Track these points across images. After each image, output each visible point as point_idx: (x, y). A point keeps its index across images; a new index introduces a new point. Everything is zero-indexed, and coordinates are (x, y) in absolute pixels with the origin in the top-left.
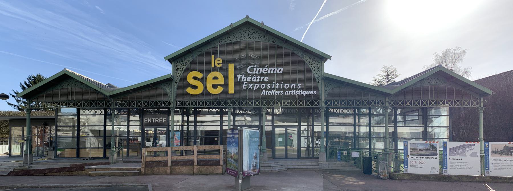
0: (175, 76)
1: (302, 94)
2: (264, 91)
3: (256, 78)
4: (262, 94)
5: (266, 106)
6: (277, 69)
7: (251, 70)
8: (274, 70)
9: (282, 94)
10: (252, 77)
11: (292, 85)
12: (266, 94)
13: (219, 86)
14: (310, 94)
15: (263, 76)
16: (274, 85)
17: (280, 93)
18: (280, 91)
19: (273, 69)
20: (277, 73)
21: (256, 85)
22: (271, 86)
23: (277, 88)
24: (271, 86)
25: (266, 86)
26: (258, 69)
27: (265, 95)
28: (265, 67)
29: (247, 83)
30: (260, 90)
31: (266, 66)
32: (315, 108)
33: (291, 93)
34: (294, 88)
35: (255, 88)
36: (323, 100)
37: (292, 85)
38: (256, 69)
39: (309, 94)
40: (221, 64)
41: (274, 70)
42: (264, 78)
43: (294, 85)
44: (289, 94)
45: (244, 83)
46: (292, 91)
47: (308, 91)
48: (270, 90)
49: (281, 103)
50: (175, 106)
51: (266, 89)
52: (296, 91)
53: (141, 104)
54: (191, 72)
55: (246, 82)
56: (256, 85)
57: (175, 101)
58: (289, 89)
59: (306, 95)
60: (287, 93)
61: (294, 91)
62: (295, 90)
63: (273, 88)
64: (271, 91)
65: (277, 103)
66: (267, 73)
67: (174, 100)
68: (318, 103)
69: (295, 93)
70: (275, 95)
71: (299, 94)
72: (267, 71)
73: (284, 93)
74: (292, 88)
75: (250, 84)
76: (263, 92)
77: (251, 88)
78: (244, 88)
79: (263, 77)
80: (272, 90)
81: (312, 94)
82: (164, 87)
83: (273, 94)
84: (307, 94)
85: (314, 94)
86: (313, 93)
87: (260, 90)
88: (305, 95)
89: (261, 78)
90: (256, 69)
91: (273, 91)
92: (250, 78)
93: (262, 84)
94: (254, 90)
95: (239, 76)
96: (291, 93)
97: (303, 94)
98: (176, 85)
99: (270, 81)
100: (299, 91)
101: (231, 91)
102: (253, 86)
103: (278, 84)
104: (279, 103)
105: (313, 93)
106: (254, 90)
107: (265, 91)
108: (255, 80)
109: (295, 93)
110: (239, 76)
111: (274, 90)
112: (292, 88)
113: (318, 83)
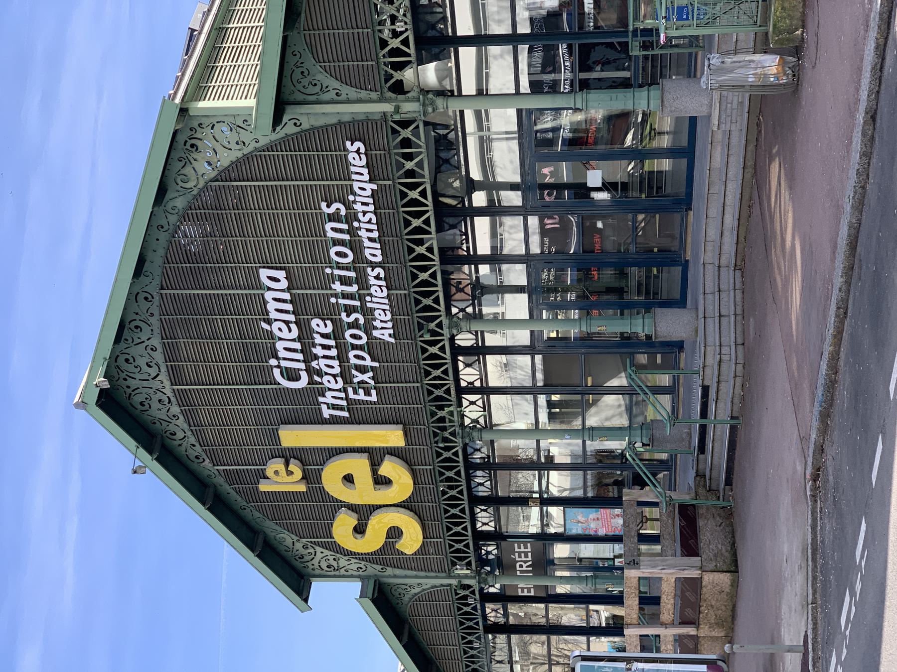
0: (361, 573)
1: (373, 196)
2: (375, 333)
3: (323, 362)
4: (392, 340)
5: (443, 319)
6: (269, 289)
7: (292, 375)
8: (275, 299)
9: (378, 270)
10: (320, 373)
11: (331, 234)
12: (390, 325)
13: (380, 473)
14: (368, 165)
15: (313, 338)
16: (339, 268)
17: (377, 277)
18: (367, 280)
19: (272, 306)
20: (289, 289)
21: (354, 361)
22: (350, 310)
23: (354, 288)
24: (350, 310)
25: (355, 325)
26: (282, 354)
27: (393, 328)
28: (271, 332)
29: (350, 390)
30: (373, 348)
31: (265, 326)
32: (437, 204)
33: (371, 240)
34: (345, 227)
35: (368, 362)
36: (388, 108)
37: (331, 234)
38: (284, 359)
39: (365, 171)
40: (287, 464)
41: (275, 299)
42: (318, 333)
43: (332, 229)
44: (378, 246)
45: (351, 395)
46: (363, 233)
47: (349, 173)
48: (368, 313)
49: (400, 66)
50: (473, 575)
51: (368, 328)
52: (359, 221)
53: (468, 605)
54: (332, 537)
55: (345, 390)
56: (354, 361)
57: (452, 574)
58: (356, 246)
59: (371, 181)
60: (373, 252)
61: (359, 228)
62: (356, 224)
63: (357, 303)
64: (375, 309)
65: (442, 419)
66: (296, 323)
67: (449, 576)
68: (405, 124)
69: (370, 222)
70: (388, 297)
71: (371, 208)
72: (287, 323)
73: (374, 266)
74: (347, 237)
75: (356, 380)
76: (384, 334)
77: (371, 374)
78: (374, 397)
79: (316, 336)
80: (369, 305)
81: (363, 156)
82: (406, 599)
83: (386, 301)
84: (366, 177)
85: (363, 150)
86: (358, 151)
87: (373, 348)
88: (375, 187)
89: (320, 345)
90: (284, 359)
91: (371, 302)
92: (326, 378)
93: (348, 361)
94: (376, 364)
95: (326, 413)
96: (371, 240)
97: (369, 193)
98: (390, 571)
99: (329, 313)
100: (358, 207)
101: (394, 437)
102: (362, 370)
103: (338, 287)
104: (441, 414)
105: (358, 151)
106: (376, 364)
107: (375, 328)
108: (335, 363)
109: (370, 222)
110: (326, 413)
111: (368, 298)
112: (347, 237)
113: (306, 126)
